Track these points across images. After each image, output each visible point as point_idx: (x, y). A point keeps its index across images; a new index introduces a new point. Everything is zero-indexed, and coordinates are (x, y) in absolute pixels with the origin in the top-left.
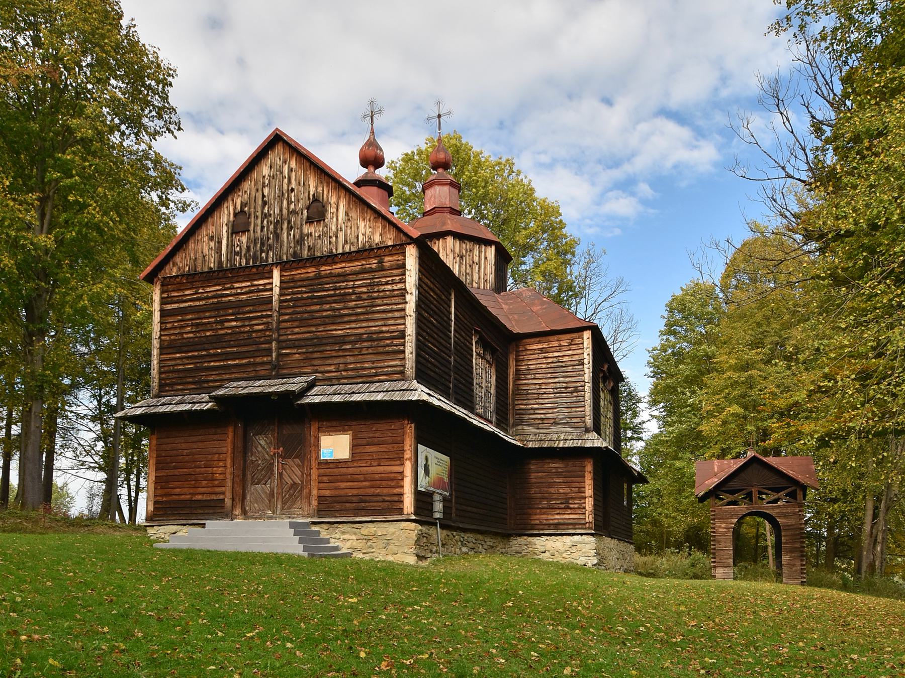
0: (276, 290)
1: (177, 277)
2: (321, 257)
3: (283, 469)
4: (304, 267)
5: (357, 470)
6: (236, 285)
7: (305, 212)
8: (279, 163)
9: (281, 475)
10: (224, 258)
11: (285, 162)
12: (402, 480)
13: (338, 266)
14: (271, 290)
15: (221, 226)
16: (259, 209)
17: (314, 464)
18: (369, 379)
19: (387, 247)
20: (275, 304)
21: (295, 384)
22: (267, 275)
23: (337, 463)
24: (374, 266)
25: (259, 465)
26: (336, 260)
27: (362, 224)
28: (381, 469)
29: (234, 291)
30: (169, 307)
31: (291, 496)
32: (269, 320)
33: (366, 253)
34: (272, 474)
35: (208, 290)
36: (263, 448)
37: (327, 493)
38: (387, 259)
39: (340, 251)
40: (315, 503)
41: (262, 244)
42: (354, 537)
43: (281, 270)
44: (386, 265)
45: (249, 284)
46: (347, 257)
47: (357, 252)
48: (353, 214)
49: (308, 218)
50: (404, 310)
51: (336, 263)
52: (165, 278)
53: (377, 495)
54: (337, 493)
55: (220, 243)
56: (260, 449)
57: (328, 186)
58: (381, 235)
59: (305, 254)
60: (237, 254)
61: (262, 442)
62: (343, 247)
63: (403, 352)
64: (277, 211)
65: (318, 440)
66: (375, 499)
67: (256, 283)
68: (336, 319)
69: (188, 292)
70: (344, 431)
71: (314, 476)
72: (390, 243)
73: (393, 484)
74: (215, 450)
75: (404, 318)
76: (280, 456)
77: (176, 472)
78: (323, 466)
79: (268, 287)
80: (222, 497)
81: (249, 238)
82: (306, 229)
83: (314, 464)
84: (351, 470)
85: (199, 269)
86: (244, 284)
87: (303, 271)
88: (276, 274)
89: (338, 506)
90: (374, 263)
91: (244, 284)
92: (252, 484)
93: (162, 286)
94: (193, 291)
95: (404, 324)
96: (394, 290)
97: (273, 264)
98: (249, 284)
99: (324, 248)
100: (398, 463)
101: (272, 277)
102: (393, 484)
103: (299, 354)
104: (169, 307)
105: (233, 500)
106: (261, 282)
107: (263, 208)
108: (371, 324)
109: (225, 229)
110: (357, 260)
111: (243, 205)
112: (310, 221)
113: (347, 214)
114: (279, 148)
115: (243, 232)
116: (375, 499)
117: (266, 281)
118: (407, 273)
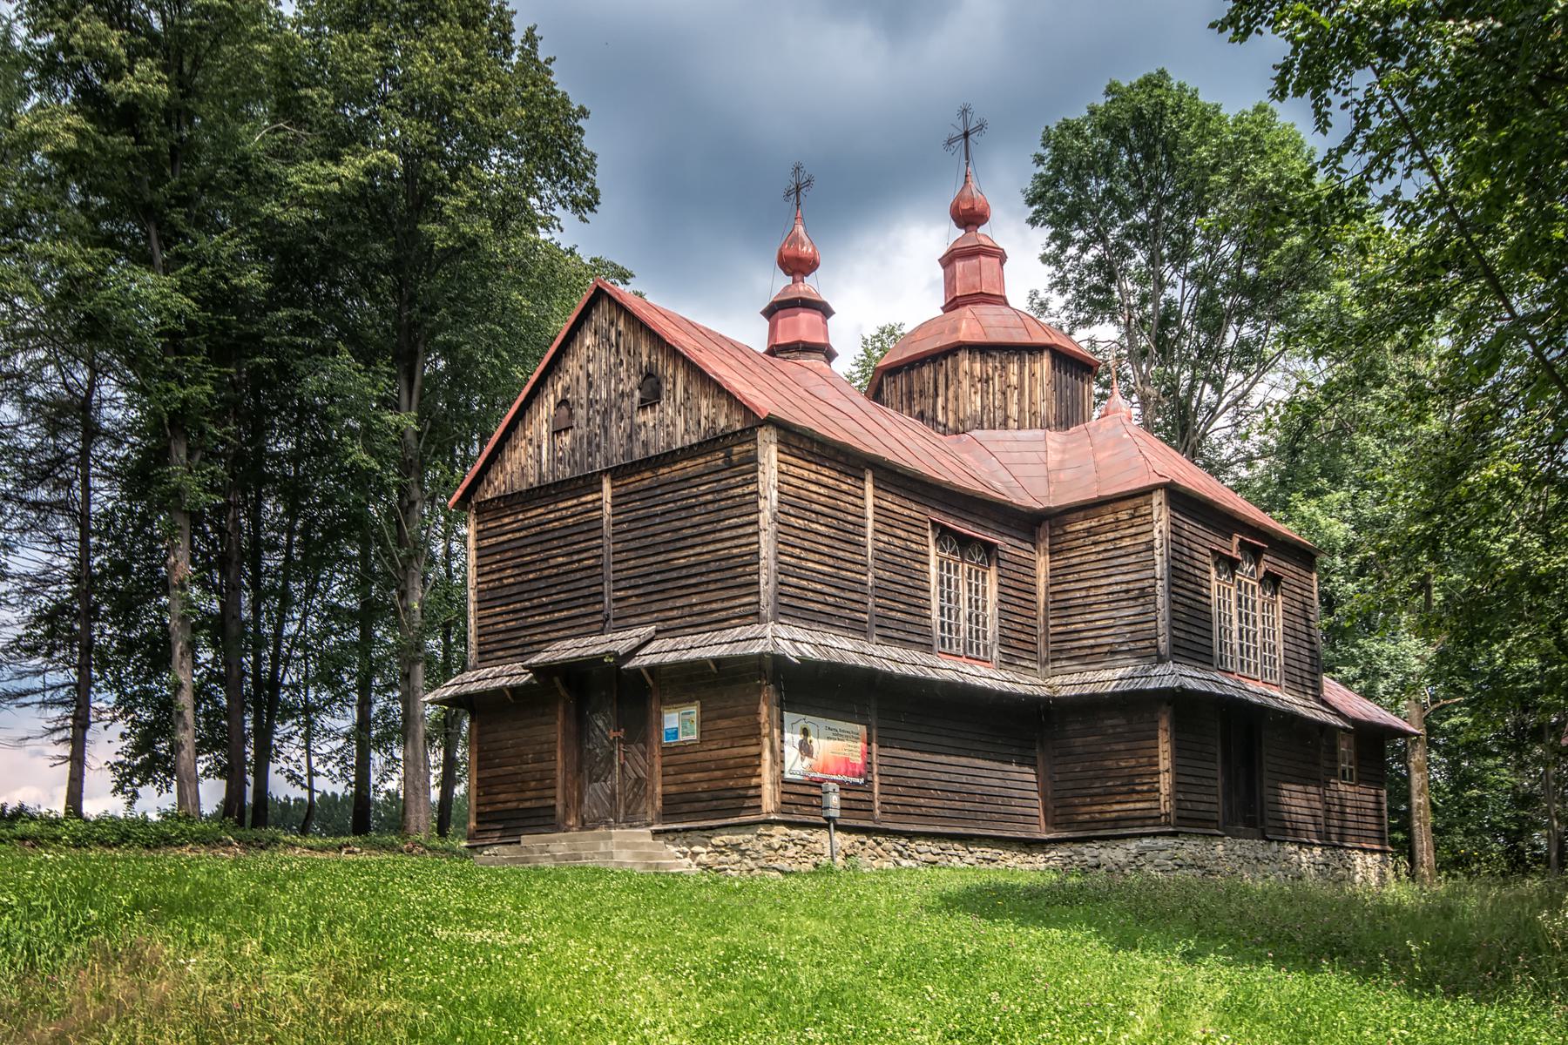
0: (608, 509)
1: (492, 500)
2: (657, 457)
3: (626, 758)
4: (639, 473)
5: (708, 755)
6: (561, 505)
7: (637, 393)
8: (605, 325)
9: (623, 767)
10: (544, 469)
11: (612, 323)
12: (760, 765)
13: (679, 466)
14: (601, 508)
15: (541, 424)
16: (584, 394)
17: (657, 751)
18: (720, 624)
19: (735, 433)
20: (607, 530)
21: (620, 642)
22: (596, 487)
23: (684, 748)
24: (720, 462)
25: (597, 755)
26: (676, 458)
27: (704, 403)
28: (735, 751)
29: (558, 514)
30: (486, 543)
31: (635, 795)
32: (599, 551)
33: (710, 447)
34: (613, 766)
35: (529, 515)
36: (601, 730)
37: (673, 789)
38: (736, 449)
39: (679, 445)
40: (658, 803)
41: (589, 443)
42: (704, 850)
43: (613, 479)
44: (735, 458)
45: (575, 502)
46: (689, 452)
47: (700, 444)
48: (694, 389)
49: (642, 401)
50: (756, 522)
51: (675, 463)
52: (479, 504)
53: (732, 789)
54: (684, 788)
55: (539, 447)
56: (597, 732)
57: (662, 353)
58: (727, 416)
59: (638, 453)
60: (560, 460)
61: (600, 723)
62: (683, 438)
63: (758, 583)
64: (604, 395)
65: (660, 715)
66: (728, 794)
67: (583, 499)
68: (675, 544)
69: (506, 520)
70: (690, 701)
71: (658, 768)
72: (738, 427)
73: (748, 771)
74: (543, 739)
75: (756, 533)
76: (621, 741)
77: (500, 771)
78: (667, 752)
79: (598, 504)
80: (552, 802)
81: (574, 438)
82: (640, 419)
83: (657, 751)
84: (700, 756)
85: (517, 488)
86: (570, 503)
87: (638, 478)
88: (607, 485)
89: (686, 808)
90: (718, 459)
91: (570, 503)
92: (590, 782)
93: (477, 514)
94: (511, 519)
95: (758, 543)
96: (744, 495)
97: (601, 472)
98: (575, 502)
99: (659, 445)
100: (754, 741)
101: (601, 490)
102: (748, 771)
103: (636, 596)
104: (486, 543)
105: (566, 806)
106: (590, 498)
107: (588, 393)
108: (719, 546)
109: (545, 425)
110: (701, 455)
111: (566, 390)
112: (643, 405)
113: (686, 390)
114: (604, 305)
115: (566, 430)
116: (728, 794)
117: (595, 496)
118: (761, 468)
